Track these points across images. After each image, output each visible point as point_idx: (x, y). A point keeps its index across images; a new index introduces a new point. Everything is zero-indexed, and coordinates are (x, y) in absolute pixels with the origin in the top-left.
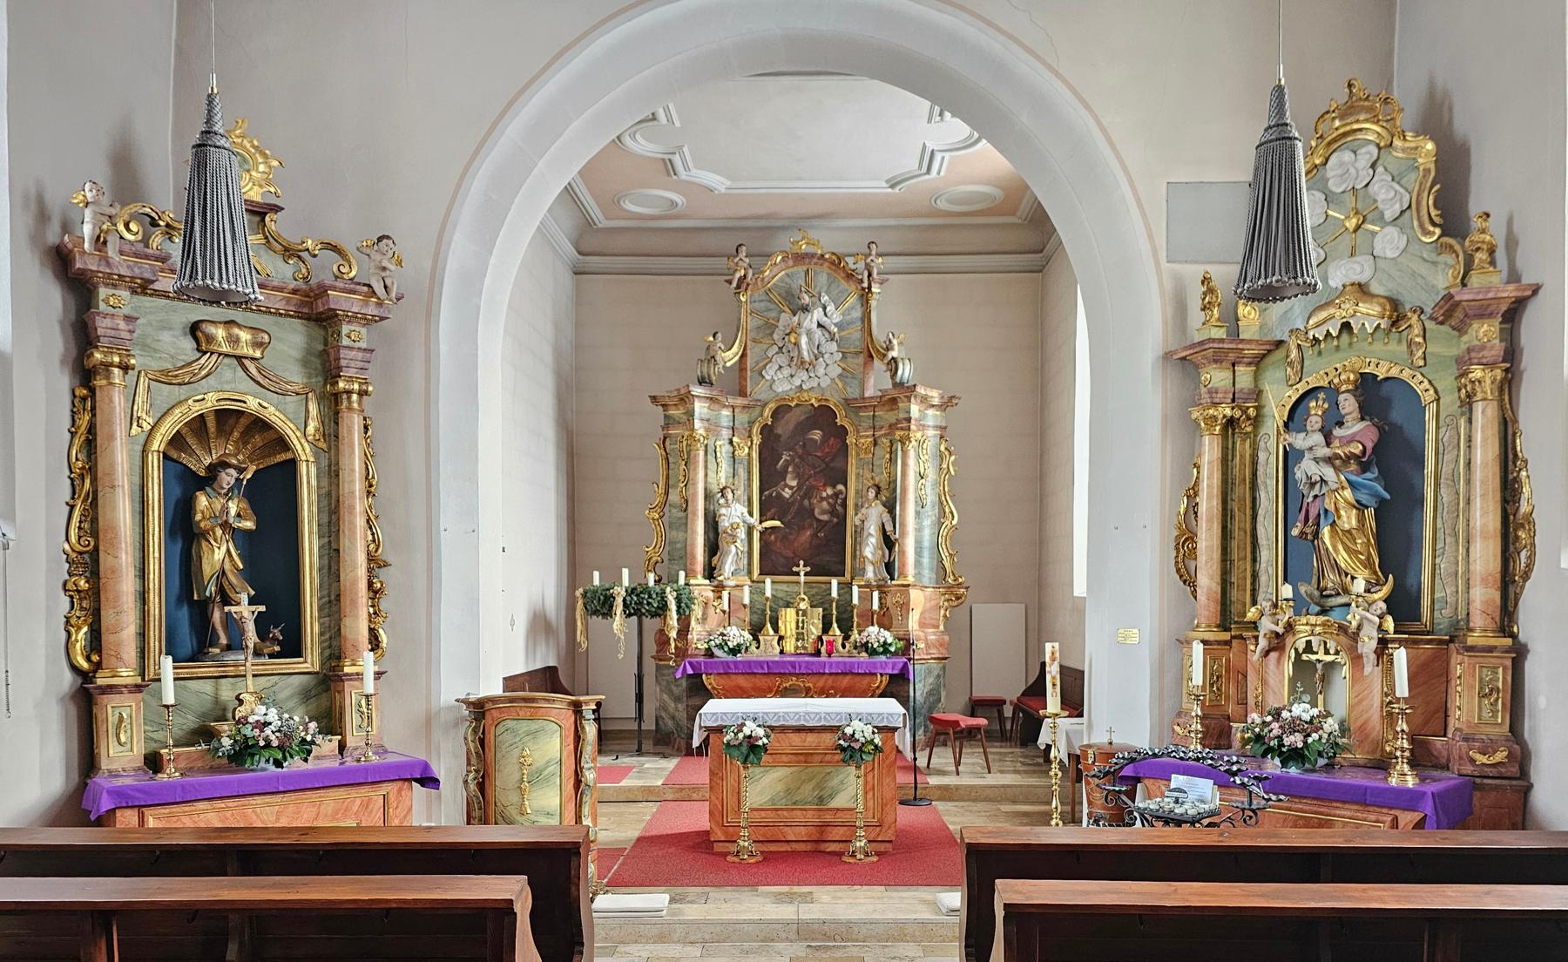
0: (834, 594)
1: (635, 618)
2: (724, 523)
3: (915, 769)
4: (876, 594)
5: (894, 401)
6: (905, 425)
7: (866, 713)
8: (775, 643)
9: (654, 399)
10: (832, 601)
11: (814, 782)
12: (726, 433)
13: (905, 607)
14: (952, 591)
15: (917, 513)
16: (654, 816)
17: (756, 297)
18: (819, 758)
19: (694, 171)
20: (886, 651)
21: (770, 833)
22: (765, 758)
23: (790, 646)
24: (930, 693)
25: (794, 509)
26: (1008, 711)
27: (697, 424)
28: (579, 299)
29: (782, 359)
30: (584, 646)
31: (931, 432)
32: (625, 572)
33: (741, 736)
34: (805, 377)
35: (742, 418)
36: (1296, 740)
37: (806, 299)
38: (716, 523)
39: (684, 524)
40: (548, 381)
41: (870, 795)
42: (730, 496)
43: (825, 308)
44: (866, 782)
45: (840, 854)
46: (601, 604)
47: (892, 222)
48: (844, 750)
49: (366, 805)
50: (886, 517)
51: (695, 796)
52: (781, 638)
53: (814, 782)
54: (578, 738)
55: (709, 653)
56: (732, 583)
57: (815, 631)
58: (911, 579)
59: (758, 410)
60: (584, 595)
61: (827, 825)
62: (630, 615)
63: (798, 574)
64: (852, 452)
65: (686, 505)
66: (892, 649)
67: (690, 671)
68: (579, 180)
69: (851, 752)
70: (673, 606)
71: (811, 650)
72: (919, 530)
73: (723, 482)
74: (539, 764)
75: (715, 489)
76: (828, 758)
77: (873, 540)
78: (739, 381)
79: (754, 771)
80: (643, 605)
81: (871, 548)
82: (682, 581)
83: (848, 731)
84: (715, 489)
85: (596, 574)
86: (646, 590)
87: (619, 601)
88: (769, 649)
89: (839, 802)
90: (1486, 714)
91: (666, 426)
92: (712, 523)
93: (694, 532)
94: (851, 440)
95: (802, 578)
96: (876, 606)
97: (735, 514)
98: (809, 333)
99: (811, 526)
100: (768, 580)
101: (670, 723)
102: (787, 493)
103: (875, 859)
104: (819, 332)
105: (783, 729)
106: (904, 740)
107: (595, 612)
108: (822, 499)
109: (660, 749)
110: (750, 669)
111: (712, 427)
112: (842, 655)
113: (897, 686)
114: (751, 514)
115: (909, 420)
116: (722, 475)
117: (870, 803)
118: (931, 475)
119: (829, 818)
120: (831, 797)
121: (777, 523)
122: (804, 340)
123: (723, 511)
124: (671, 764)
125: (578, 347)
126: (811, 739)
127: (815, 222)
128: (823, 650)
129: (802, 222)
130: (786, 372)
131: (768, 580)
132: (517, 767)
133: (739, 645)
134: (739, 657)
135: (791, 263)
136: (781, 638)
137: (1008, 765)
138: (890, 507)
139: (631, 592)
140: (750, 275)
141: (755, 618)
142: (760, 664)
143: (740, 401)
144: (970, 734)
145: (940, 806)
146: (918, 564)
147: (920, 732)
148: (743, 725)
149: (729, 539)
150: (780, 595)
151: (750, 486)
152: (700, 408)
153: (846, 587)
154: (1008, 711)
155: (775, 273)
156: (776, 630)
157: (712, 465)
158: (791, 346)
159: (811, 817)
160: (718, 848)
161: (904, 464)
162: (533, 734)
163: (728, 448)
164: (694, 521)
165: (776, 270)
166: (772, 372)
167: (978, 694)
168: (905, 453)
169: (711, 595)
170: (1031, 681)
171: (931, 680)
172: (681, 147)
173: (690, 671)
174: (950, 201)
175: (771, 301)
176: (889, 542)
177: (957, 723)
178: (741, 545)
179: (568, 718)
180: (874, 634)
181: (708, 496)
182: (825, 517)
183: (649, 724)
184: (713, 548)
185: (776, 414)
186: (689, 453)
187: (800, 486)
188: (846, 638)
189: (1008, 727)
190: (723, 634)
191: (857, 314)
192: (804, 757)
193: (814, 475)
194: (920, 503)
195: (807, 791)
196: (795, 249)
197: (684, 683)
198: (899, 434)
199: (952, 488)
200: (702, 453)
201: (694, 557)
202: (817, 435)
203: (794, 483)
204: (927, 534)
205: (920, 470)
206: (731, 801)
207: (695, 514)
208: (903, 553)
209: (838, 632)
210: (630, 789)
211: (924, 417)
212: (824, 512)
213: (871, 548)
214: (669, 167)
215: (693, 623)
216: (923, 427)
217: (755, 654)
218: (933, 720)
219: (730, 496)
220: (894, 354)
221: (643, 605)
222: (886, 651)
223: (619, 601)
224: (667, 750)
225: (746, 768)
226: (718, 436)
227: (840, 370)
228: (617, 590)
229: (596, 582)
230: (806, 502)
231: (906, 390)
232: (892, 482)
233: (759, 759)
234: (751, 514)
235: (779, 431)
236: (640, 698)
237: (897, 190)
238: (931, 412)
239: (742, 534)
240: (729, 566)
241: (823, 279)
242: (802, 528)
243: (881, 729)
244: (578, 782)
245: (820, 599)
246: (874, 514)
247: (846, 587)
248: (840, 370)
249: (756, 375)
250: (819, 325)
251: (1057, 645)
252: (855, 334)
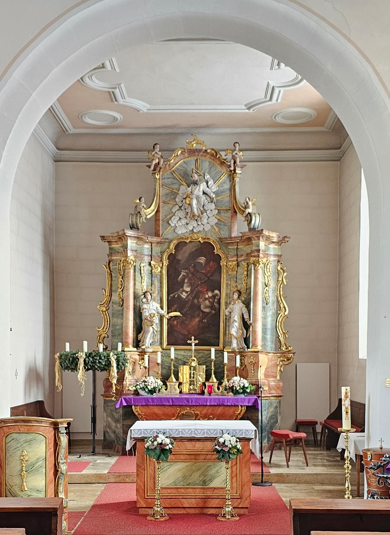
0: (213, 357)
1: (91, 371)
2: (146, 314)
3: (262, 464)
4: (238, 357)
5: (249, 239)
6: (256, 254)
7: (232, 429)
8: (177, 387)
9: (103, 238)
10: (211, 361)
11: (200, 472)
12: (147, 259)
13: (256, 365)
14: (285, 355)
15: (264, 308)
16: (102, 492)
17: (166, 176)
18: (203, 457)
19: (128, 99)
20: (244, 392)
21: (173, 503)
22: (170, 457)
23: (185, 388)
24: (271, 418)
25: (188, 305)
26: (319, 429)
27: (129, 253)
28: (57, 177)
29: (181, 214)
30: (60, 388)
31: (272, 258)
32: (85, 343)
33: (155, 443)
34: (195, 225)
35: (157, 249)
37: (196, 177)
38: (141, 314)
39: (121, 314)
40: (38, 227)
41: (234, 480)
42: (149, 297)
43: (207, 183)
44: (232, 472)
45: (216, 516)
46: (70, 363)
47: (248, 130)
48: (218, 452)
50: (245, 310)
51: (127, 480)
52: (180, 384)
53: (200, 472)
54: (56, 444)
55: (136, 393)
56: (150, 350)
57: (201, 379)
58: (259, 348)
59: (166, 245)
60: (60, 357)
61: (208, 498)
62: (88, 369)
63: (190, 345)
64: (224, 270)
65: (122, 303)
66: (248, 391)
68: (58, 105)
69: (223, 453)
70: (114, 364)
71: (198, 391)
72: (264, 318)
73: (145, 289)
74: (32, 460)
76: (209, 457)
77: (236, 324)
78: (155, 227)
79: (164, 464)
80: (96, 364)
82: (120, 349)
83: (221, 440)
84: (140, 293)
85: (68, 345)
86: (98, 354)
87: (81, 361)
88: (172, 391)
89: (216, 483)
91: (110, 255)
92: (138, 314)
93: (127, 319)
94: (223, 263)
95: (193, 347)
96: (238, 364)
97: (152, 308)
98: (198, 198)
99: (198, 315)
100: (172, 349)
101: (112, 436)
102: (184, 295)
103: (237, 518)
104: (203, 198)
105: (182, 439)
106: (255, 446)
107: (67, 368)
108: (206, 299)
109: (106, 451)
111: (139, 255)
112: (218, 394)
113: (251, 413)
114: (162, 308)
115: (258, 251)
116: (145, 284)
117: (235, 485)
118: (272, 284)
119: (209, 493)
120: (211, 480)
121: (178, 314)
122: (194, 202)
123: (145, 306)
124: (113, 460)
125: (57, 206)
126: (198, 445)
127: (202, 130)
128: (206, 391)
129: (193, 130)
130: (184, 221)
131: (172, 349)
132: (19, 462)
133: (154, 388)
135: (186, 155)
136: (180, 384)
137: (319, 462)
138: (247, 304)
139: (89, 355)
140: (162, 163)
141: (165, 371)
142: (167, 399)
143: (155, 239)
144: (296, 442)
145: (277, 486)
146: (264, 339)
147: (265, 441)
148: (157, 436)
149: (149, 323)
150: (180, 357)
152: (131, 243)
153: (220, 353)
154: (319, 429)
155: (177, 161)
156: (177, 379)
157: (138, 278)
158: (187, 206)
159: (199, 493)
160: (142, 511)
161: (256, 278)
162: (29, 442)
163: (148, 268)
164: (127, 312)
165: (177, 159)
166: (175, 222)
167: (300, 418)
168: (256, 271)
169: (137, 357)
170: (333, 410)
171: (272, 409)
172: (119, 84)
173: (125, 404)
174: (283, 118)
175: (174, 178)
176: (246, 325)
177: (287, 436)
178: (156, 327)
179: (50, 433)
180: (238, 381)
182: (207, 310)
183: (99, 436)
184: (139, 329)
185: (177, 247)
186: (124, 271)
187: (192, 291)
188: (220, 384)
189: (319, 438)
190: (145, 381)
191: (227, 186)
192: (194, 456)
193: (200, 283)
194: (265, 301)
195: (196, 477)
196: (189, 147)
197: (121, 411)
198: (252, 259)
199: (285, 292)
200: (132, 271)
201: (127, 334)
202: (202, 260)
203: (188, 289)
204: (269, 320)
205: (265, 281)
206: (150, 484)
207: (128, 308)
208: (254, 332)
209: (215, 380)
210: (88, 476)
211: (268, 249)
212: (206, 307)
213: (235, 329)
214: (112, 97)
215: (127, 375)
216: (267, 255)
217: (164, 393)
218: (273, 434)
219: (149, 297)
220: (249, 210)
221: (96, 364)
222: (244, 392)
223: (81, 361)
224: (111, 452)
225: (159, 463)
226: (142, 261)
227: (216, 221)
228: (80, 354)
229: (68, 349)
230: (196, 301)
231: (257, 233)
232: (248, 289)
233: (167, 458)
234: (162, 308)
235: (179, 257)
236: (94, 420)
237: (251, 111)
238: (272, 246)
239: (156, 320)
240: (148, 340)
241: (206, 165)
242: (193, 317)
243: (241, 440)
244: (56, 471)
245: (204, 360)
246: (238, 308)
247: (220, 353)
248: (216, 221)
249: (165, 223)
250: (204, 193)
251: (348, 388)
252: (226, 198)
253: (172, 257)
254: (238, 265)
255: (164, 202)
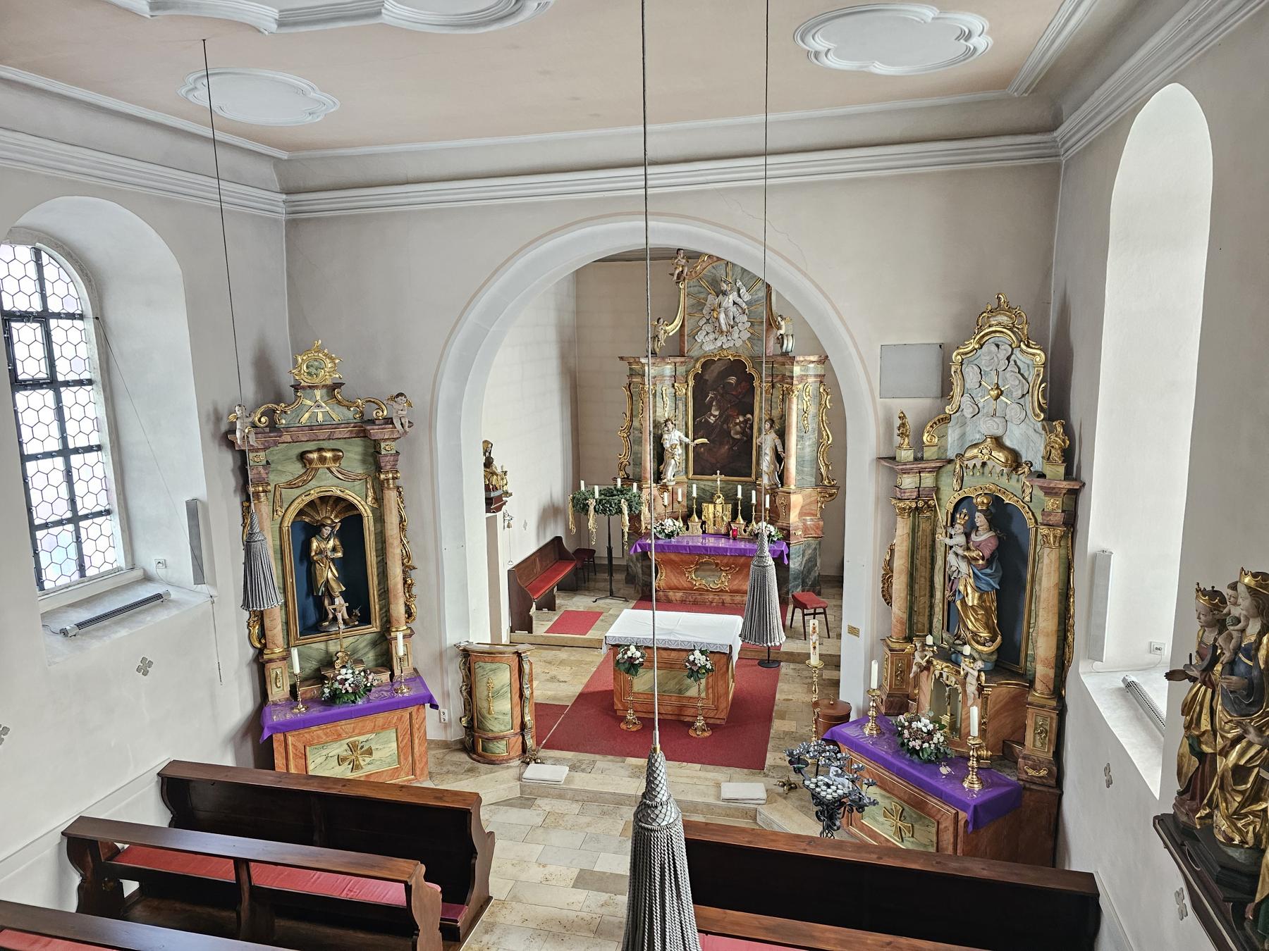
0: (739, 496)
2: (667, 445)
13: (788, 507)
29: (708, 328)
35: (681, 370)
36: (916, 744)
37: (724, 287)
49: (400, 719)
52: (704, 523)
64: (758, 392)
67: (639, 550)
71: (723, 531)
75: (662, 421)
77: (768, 458)
81: (767, 462)
88: (693, 535)
90: (1038, 744)
94: (756, 383)
102: (712, 420)
104: (733, 309)
110: (677, 549)
121: (705, 440)
122: (722, 316)
130: (712, 336)
134: (673, 540)
136: (704, 523)
143: (678, 359)
151: (687, 415)
181: (656, 425)
182: (738, 437)
185: (704, 366)
187: (720, 415)
202: (733, 380)
203: (717, 413)
204: (808, 450)
212: (737, 433)
213: (767, 462)
220: (782, 332)
231: (788, 358)
235: (707, 377)
239: (679, 450)
242: (722, 444)
245: (730, 497)
250: (735, 303)
253: (696, 376)
254: (773, 387)
255: (689, 314)
